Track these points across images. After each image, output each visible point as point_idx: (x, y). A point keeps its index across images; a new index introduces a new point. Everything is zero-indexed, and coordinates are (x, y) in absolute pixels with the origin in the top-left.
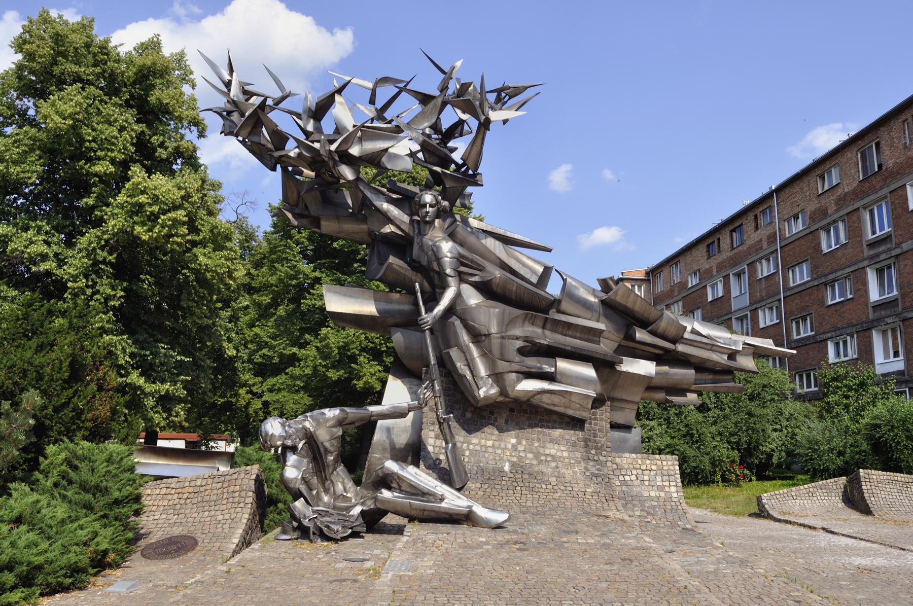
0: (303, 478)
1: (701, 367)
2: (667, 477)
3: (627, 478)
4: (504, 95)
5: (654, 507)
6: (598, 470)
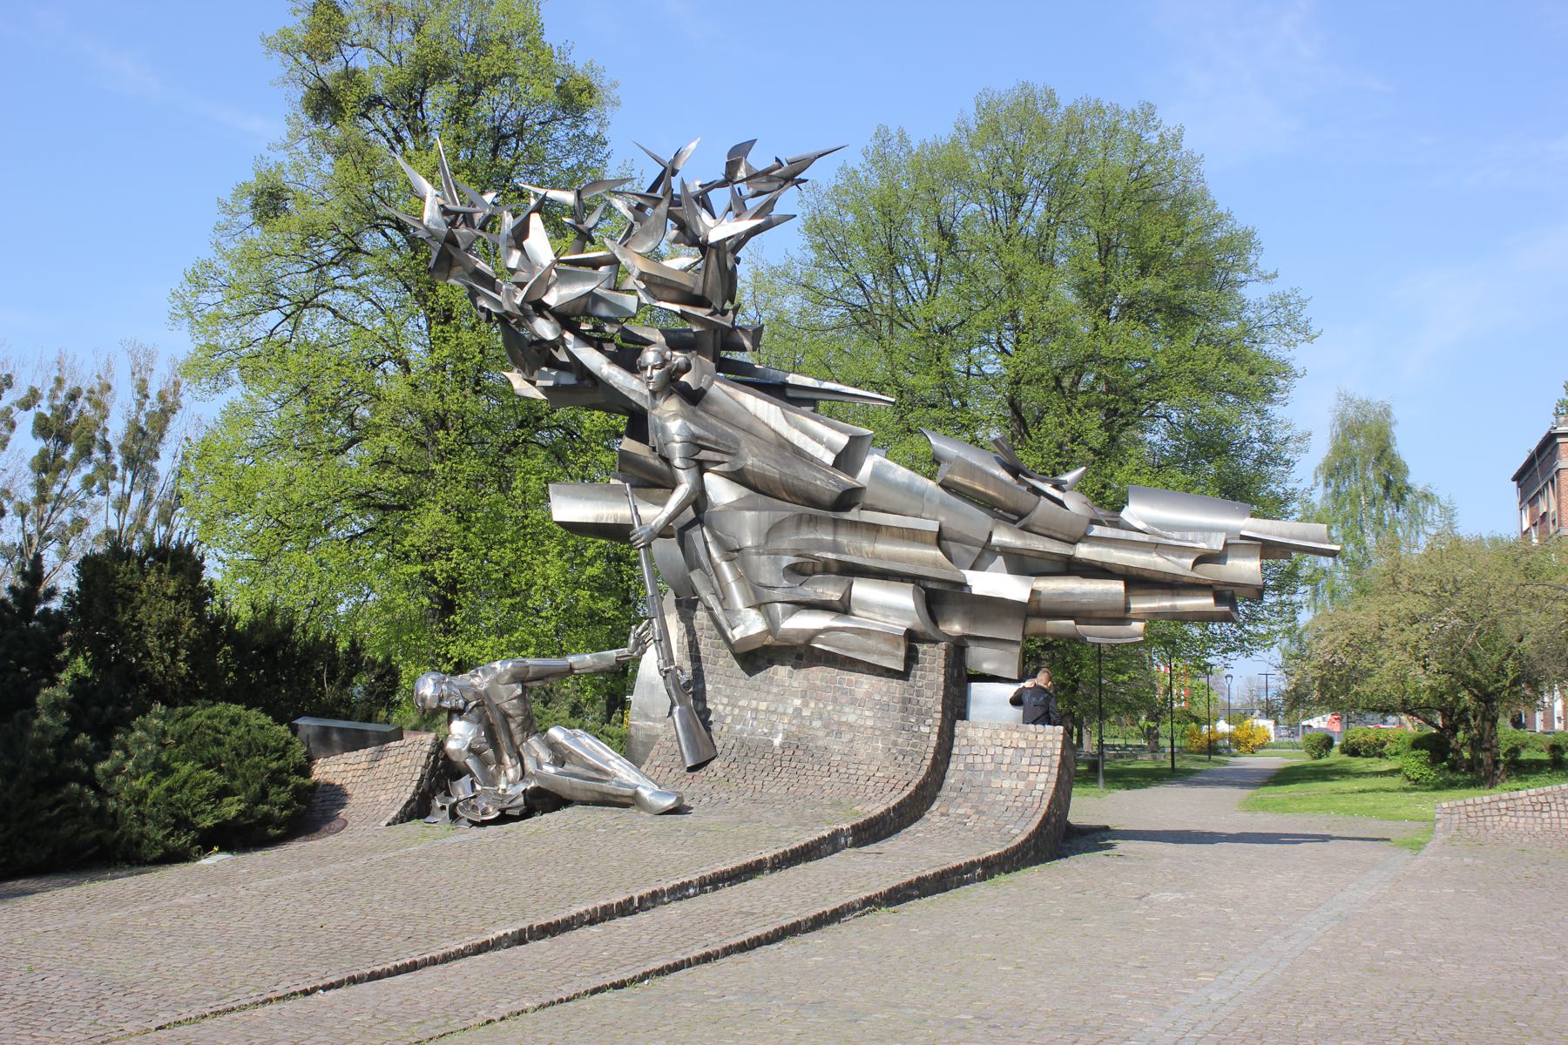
0: (470, 749)
1: (1138, 581)
2: (1038, 760)
3: (978, 759)
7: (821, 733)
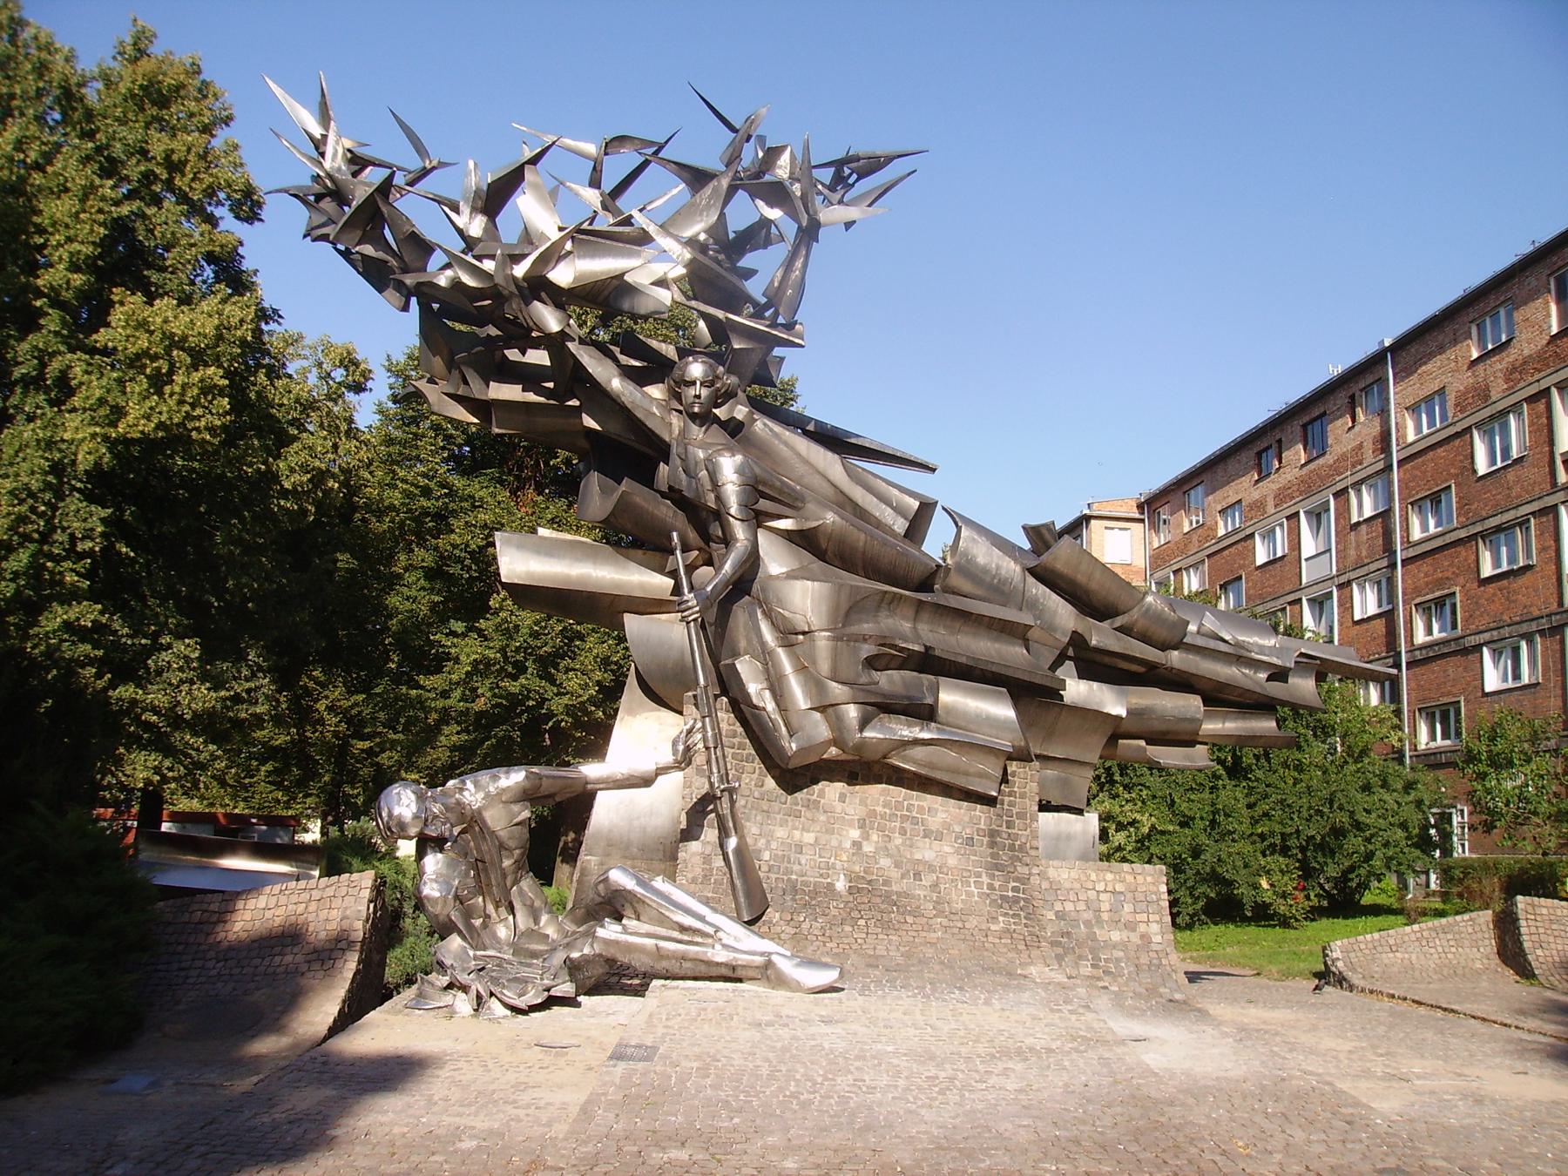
1: (1218, 697)
4: (851, 170)
5: (1118, 960)
6: (1015, 889)
7: (895, 874)
